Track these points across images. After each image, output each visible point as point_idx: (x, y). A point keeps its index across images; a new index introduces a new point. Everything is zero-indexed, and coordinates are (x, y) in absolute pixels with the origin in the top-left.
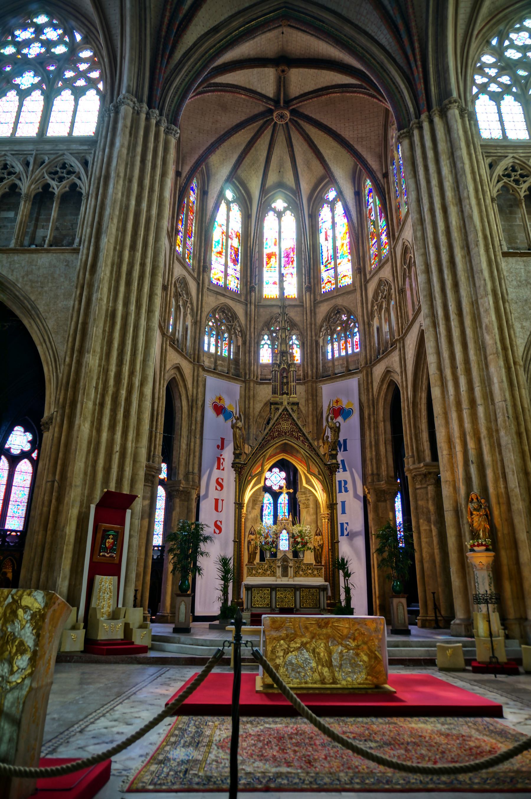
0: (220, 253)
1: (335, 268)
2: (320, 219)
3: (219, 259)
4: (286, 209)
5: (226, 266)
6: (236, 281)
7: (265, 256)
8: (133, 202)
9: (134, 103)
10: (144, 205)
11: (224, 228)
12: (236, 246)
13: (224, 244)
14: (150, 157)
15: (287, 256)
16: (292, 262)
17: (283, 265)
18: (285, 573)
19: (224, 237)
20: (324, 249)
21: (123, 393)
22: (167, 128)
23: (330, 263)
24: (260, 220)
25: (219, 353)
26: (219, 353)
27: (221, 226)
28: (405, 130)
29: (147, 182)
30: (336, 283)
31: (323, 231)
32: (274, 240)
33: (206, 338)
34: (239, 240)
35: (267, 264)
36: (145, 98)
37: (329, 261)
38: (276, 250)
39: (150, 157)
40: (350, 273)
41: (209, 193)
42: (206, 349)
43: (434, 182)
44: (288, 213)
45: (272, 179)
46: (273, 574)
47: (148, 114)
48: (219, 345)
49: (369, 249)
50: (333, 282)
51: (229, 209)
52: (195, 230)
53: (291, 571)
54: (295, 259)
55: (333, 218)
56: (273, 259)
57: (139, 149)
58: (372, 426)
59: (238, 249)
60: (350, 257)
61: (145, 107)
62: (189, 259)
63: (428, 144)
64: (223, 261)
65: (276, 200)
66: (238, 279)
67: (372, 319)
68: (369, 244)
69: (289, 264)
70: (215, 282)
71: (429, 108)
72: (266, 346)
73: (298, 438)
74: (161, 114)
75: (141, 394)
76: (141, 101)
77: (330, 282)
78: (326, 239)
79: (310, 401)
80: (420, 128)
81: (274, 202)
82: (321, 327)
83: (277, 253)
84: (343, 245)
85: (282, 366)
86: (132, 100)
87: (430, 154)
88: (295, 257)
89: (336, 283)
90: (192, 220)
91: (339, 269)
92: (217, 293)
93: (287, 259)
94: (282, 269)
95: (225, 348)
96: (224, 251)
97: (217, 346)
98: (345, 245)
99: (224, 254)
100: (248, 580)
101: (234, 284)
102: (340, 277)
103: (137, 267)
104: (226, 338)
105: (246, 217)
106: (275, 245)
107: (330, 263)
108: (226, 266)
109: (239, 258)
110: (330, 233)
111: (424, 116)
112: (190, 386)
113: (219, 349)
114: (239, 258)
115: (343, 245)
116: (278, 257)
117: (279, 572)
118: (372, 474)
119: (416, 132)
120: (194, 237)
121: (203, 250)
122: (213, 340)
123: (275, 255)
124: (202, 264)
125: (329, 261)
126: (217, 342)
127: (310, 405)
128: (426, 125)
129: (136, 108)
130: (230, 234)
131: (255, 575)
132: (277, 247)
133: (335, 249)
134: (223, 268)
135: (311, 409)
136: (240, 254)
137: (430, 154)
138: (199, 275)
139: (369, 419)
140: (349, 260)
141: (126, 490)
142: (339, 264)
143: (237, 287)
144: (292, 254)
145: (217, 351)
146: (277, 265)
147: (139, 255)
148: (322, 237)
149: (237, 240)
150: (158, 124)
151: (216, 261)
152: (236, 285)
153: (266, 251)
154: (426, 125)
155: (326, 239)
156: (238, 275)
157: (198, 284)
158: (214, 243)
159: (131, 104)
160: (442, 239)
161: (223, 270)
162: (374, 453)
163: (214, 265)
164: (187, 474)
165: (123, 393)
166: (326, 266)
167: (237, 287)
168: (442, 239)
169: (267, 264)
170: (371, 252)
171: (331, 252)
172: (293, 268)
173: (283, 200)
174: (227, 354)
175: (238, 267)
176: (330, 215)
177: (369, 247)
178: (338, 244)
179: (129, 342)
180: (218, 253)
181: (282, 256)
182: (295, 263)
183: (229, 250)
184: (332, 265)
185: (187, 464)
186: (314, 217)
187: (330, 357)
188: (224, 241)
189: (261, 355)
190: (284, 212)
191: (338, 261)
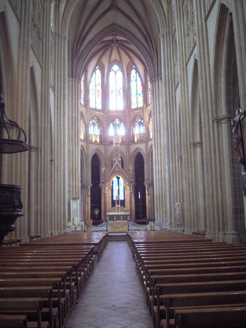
18: (118, 211)
21: (74, 171)
24: (108, 75)
36: (71, 76)
41: (88, 71)
43: (158, 103)
45: (113, 58)
46: (115, 212)
47: (72, 80)
53: (120, 211)
58: (147, 163)
71: (158, 76)
73: (121, 173)
75: (78, 170)
76: (70, 77)
79: (128, 152)
82: (132, 123)
85: (116, 148)
99: (95, 94)
100: (108, 214)
101: (99, 107)
105: (103, 75)
111: (156, 78)
112: (86, 151)
117: (116, 211)
118: (147, 179)
119: (154, 83)
127: (128, 153)
128: (157, 82)
131: (109, 212)
135: (128, 155)
139: (146, 160)
141: (77, 196)
154: (157, 82)
160: (158, 123)
162: (148, 172)
164: (87, 181)
165: (74, 171)
168: (158, 123)
179: (74, 157)
185: (87, 178)
186: (129, 74)
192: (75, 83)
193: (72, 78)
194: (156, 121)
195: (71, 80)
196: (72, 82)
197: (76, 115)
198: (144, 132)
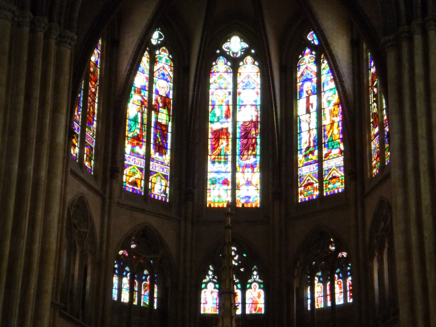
0: (138, 138)
1: (320, 161)
2: (299, 74)
3: (137, 149)
4: (247, 52)
5: (148, 158)
6: (164, 182)
7: (210, 136)
8: (16, 167)
9: (13, 12)
10: (31, 167)
11: (145, 93)
12: (164, 122)
13: (145, 121)
14: (37, 93)
15: (246, 135)
16: (254, 145)
17: (238, 152)
19: (146, 110)
20: (304, 126)
22: (60, 36)
23: (312, 153)
25: (135, 303)
26: (135, 303)
27: (139, 92)
28: (391, 37)
29: (34, 132)
30: (321, 189)
31: (305, 95)
32: (225, 108)
33: (115, 280)
34: (169, 110)
35: (214, 149)
37: (311, 149)
38: (228, 125)
39: (37, 93)
40: (340, 174)
42: (115, 297)
44: (249, 59)
47: (32, 23)
48: (136, 289)
49: (370, 141)
50: (316, 185)
51: (153, 61)
52: (98, 110)
54: (258, 141)
55: (319, 74)
56: (223, 143)
57: (22, 84)
59: (166, 126)
60: (342, 147)
61: (29, 15)
62: (89, 160)
63: (419, 70)
64: (142, 151)
65: (230, 38)
66: (165, 177)
67: (372, 259)
68: (370, 132)
69: (248, 150)
70: (129, 188)
72: (211, 286)
74: (51, 20)
77: (311, 184)
78: (308, 112)
80: (411, 40)
81: (226, 41)
83: (230, 130)
84: (332, 124)
86: (10, 10)
87: (420, 86)
88: (258, 137)
89: (321, 189)
90: (94, 94)
91: (326, 165)
92: (133, 209)
93: (245, 141)
94: (238, 157)
95: (145, 293)
96: (144, 134)
97: (131, 291)
98: (336, 125)
102: (326, 177)
103: (22, 262)
104: (146, 276)
106: (227, 117)
107: (312, 153)
108: (148, 158)
109: (169, 141)
110: (313, 99)
113: (136, 296)
114: (169, 141)
115: (332, 124)
116: (231, 136)
119: (405, 46)
120: (97, 121)
121: (111, 141)
122: (126, 281)
123: (227, 133)
124: (109, 166)
125: (311, 149)
126: (132, 284)
128: (418, 39)
129: (16, 19)
130: (154, 103)
132: (230, 120)
133: (320, 128)
134: (141, 163)
136: (169, 135)
137: (420, 86)
138: (104, 184)
140: (341, 152)
142: (327, 155)
143: (165, 192)
144: (253, 132)
145: (131, 298)
146: (229, 152)
147: (23, 243)
148: (301, 105)
149: (165, 111)
150: (47, 36)
151: (132, 152)
152: (163, 188)
153: (214, 126)
154: (418, 39)
155: (308, 112)
156: (167, 171)
157: (103, 199)
158: (128, 122)
159: (10, 15)
161: (143, 167)
163: (129, 160)
166: (305, 156)
167: (165, 192)
169: (214, 149)
170: (373, 146)
171: (314, 133)
172: (255, 156)
173: (241, 38)
174: (147, 303)
175: (167, 158)
176: (314, 68)
177: (370, 137)
178: (326, 122)
180: (134, 138)
181: (238, 135)
182: (258, 147)
183: (152, 130)
184: (315, 157)
187: (309, 309)
188: (145, 116)
189: (203, 301)
190: (242, 58)
191: (325, 151)
192: (47, 36)
193: (34, 11)
194: (413, 209)
195: (27, 20)
196: (33, 31)
197: (43, 173)
198: (350, 301)
